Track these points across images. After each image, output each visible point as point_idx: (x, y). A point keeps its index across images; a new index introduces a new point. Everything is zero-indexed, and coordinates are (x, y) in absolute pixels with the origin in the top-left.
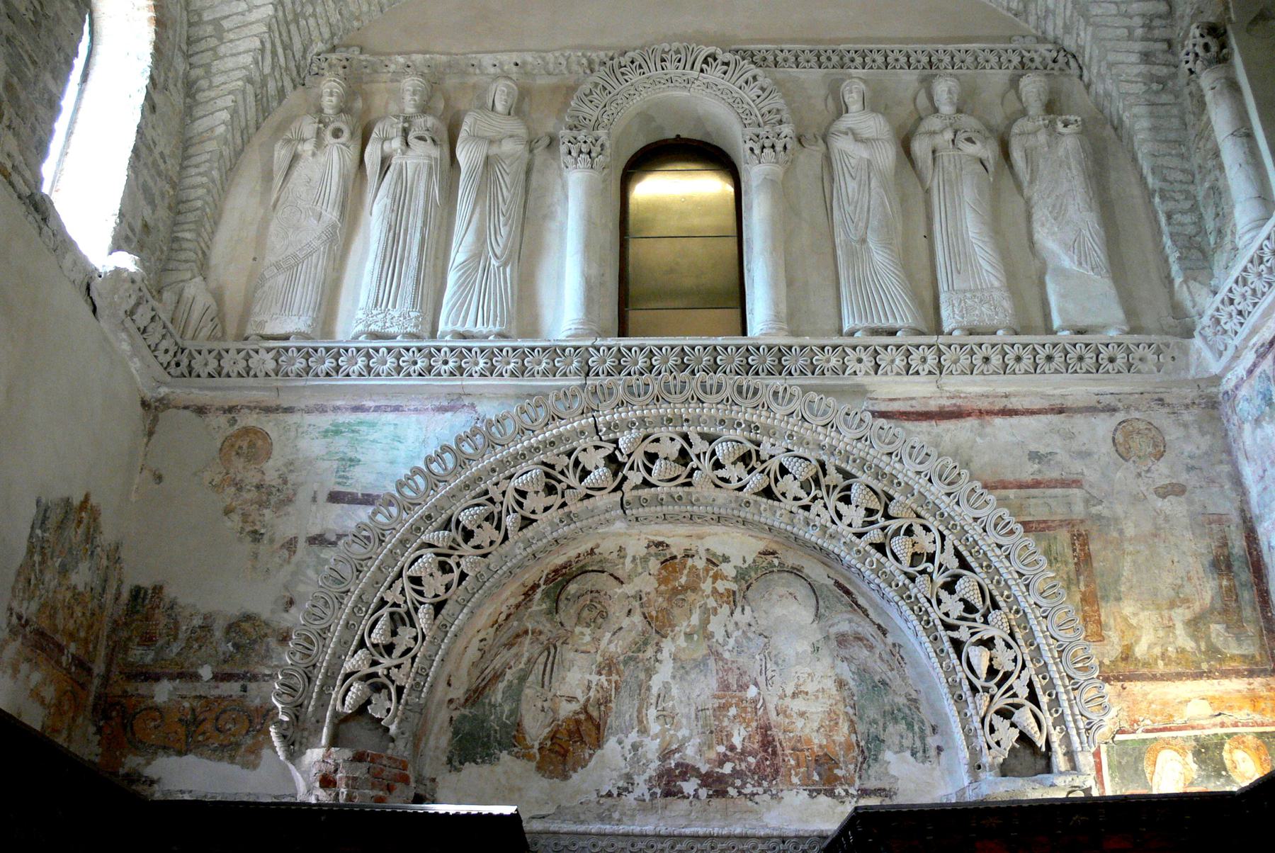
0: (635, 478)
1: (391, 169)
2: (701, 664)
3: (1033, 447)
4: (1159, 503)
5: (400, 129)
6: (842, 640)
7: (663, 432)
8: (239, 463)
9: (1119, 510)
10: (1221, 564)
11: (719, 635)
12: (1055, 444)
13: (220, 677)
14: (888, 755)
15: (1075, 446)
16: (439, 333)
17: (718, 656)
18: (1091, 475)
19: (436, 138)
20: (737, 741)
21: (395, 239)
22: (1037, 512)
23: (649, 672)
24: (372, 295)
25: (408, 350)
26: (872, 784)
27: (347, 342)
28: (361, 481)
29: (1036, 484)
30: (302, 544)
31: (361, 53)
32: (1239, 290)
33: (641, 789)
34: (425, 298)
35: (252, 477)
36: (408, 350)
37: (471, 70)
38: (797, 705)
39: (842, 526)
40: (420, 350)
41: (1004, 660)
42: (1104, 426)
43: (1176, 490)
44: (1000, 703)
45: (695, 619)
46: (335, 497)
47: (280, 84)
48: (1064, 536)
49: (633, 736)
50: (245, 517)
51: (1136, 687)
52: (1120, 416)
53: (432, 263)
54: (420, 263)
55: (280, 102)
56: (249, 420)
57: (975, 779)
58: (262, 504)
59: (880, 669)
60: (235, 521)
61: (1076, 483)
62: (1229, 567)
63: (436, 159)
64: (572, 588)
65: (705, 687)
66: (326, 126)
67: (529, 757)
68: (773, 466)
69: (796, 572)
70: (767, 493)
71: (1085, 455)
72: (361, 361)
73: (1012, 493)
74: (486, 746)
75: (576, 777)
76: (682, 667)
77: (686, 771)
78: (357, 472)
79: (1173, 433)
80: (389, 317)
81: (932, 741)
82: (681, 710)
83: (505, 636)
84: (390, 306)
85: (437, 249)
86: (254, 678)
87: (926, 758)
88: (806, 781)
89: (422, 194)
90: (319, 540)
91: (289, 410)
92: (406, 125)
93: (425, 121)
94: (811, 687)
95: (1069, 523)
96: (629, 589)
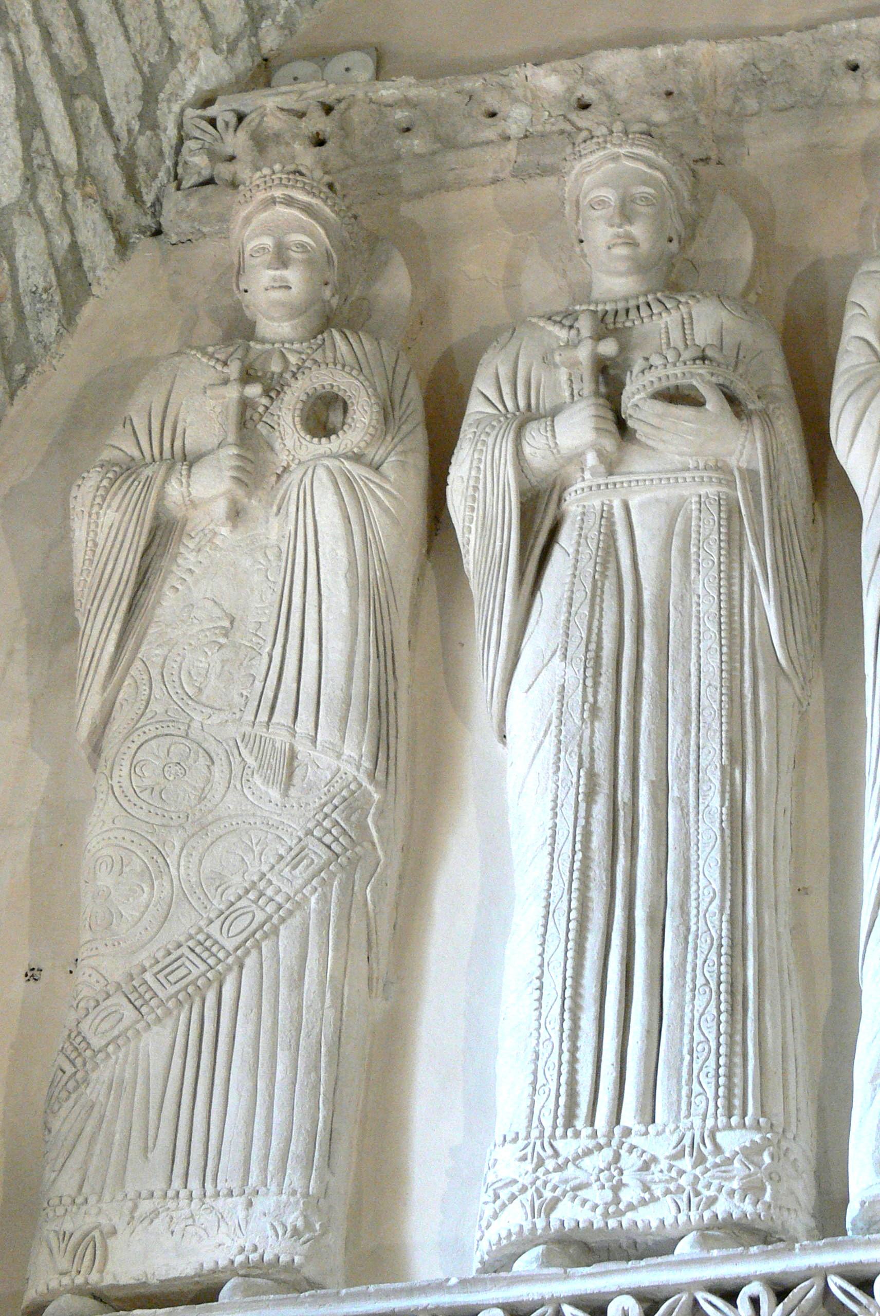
1: (566, 538)
5: (586, 370)
16: (852, 1211)
19: (740, 388)
24: (549, 1079)
25: (730, 1295)
27: (465, 1284)
31: (379, 74)
34: (774, 1064)
36: (730, 1295)
37: (849, 86)
40: (781, 1292)
47: (62, 241)
53: (785, 917)
54: (736, 922)
55: (69, 319)
63: (750, 476)
66: (273, 390)
80: (630, 1162)
84: (629, 1116)
85: (797, 851)
89: (711, 628)
92: (608, 348)
93: (686, 324)
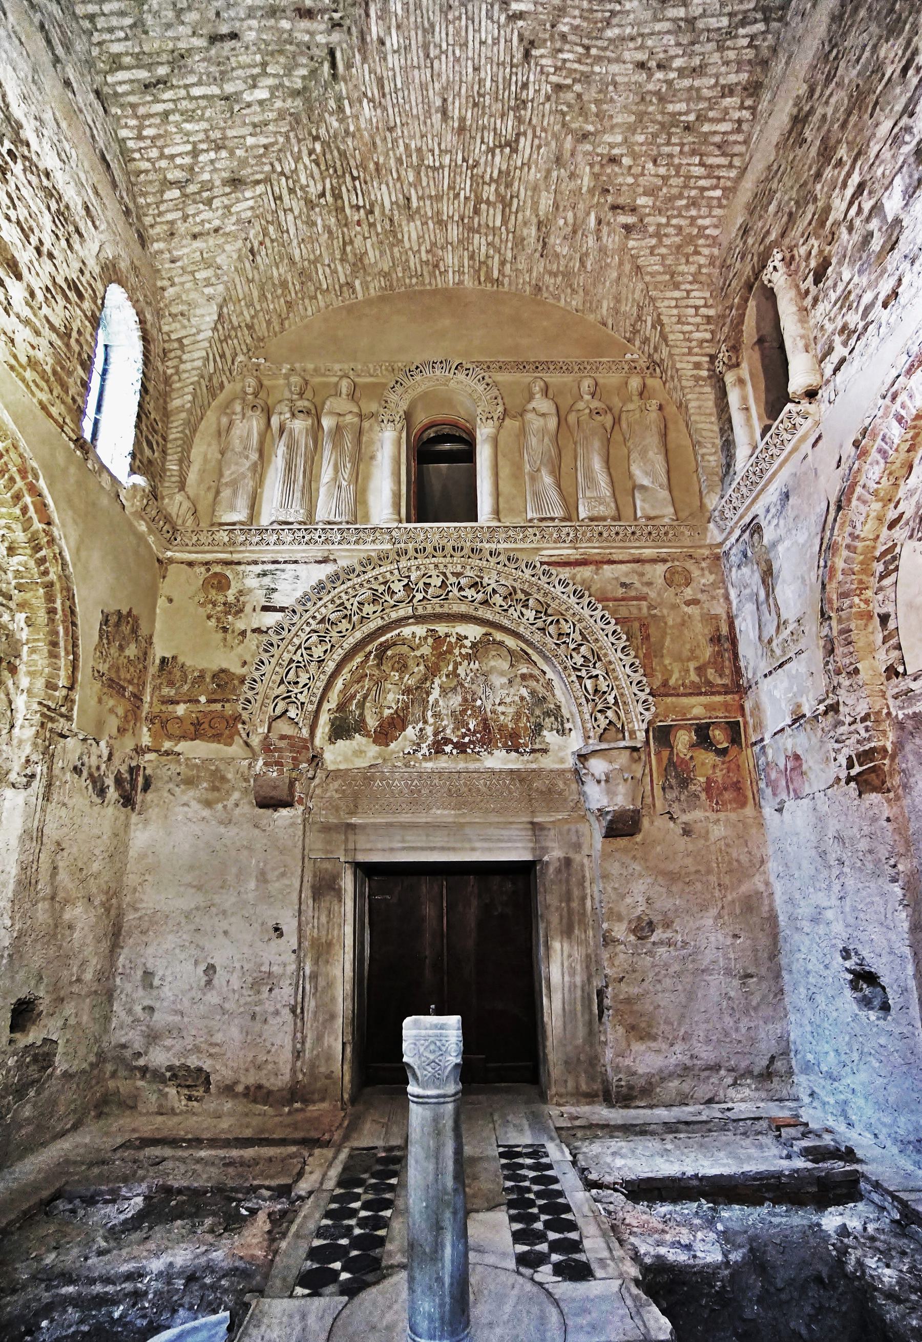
0: (419, 596)
2: (454, 690)
3: (623, 580)
4: (686, 609)
6: (524, 677)
7: (434, 573)
8: (214, 592)
9: (665, 612)
10: (716, 639)
11: (463, 675)
12: (635, 579)
13: (210, 701)
14: (545, 733)
15: (645, 579)
17: (462, 685)
18: (652, 595)
20: (471, 726)
21: (290, 470)
22: (623, 612)
23: (428, 694)
26: (537, 747)
28: (279, 600)
29: (623, 599)
30: (249, 633)
32: (734, 495)
33: (425, 750)
35: (221, 599)
38: (501, 709)
39: (524, 620)
41: (603, 686)
42: (661, 568)
43: (695, 602)
44: (599, 707)
45: (451, 668)
46: (265, 609)
48: (636, 625)
49: (420, 725)
50: (218, 620)
51: (669, 700)
52: (669, 564)
56: (217, 569)
57: (587, 744)
58: (227, 613)
59: (541, 691)
60: (212, 623)
61: (644, 598)
62: (719, 640)
64: (389, 653)
65: (456, 701)
67: (368, 735)
68: (490, 589)
69: (501, 644)
70: (485, 602)
71: (649, 584)
72: (275, 537)
73: (611, 604)
74: (348, 731)
75: (392, 745)
76: (444, 691)
77: (447, 741)
78: (275, 596)
79: (696, 573)
81: (567, 726)
82: (444, 712)
83: (355, 678)
86: (228, 701)
87: (563, 734)
88: (505, 746)
90: (257, 630)
91: (239, 563)
94: (508, 700)
95: (639, 619)
96: (418, 653)
